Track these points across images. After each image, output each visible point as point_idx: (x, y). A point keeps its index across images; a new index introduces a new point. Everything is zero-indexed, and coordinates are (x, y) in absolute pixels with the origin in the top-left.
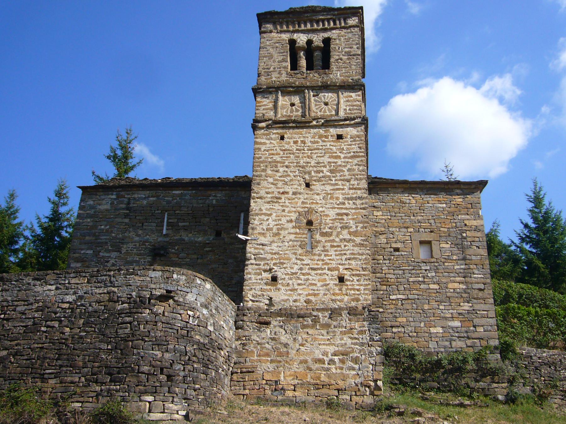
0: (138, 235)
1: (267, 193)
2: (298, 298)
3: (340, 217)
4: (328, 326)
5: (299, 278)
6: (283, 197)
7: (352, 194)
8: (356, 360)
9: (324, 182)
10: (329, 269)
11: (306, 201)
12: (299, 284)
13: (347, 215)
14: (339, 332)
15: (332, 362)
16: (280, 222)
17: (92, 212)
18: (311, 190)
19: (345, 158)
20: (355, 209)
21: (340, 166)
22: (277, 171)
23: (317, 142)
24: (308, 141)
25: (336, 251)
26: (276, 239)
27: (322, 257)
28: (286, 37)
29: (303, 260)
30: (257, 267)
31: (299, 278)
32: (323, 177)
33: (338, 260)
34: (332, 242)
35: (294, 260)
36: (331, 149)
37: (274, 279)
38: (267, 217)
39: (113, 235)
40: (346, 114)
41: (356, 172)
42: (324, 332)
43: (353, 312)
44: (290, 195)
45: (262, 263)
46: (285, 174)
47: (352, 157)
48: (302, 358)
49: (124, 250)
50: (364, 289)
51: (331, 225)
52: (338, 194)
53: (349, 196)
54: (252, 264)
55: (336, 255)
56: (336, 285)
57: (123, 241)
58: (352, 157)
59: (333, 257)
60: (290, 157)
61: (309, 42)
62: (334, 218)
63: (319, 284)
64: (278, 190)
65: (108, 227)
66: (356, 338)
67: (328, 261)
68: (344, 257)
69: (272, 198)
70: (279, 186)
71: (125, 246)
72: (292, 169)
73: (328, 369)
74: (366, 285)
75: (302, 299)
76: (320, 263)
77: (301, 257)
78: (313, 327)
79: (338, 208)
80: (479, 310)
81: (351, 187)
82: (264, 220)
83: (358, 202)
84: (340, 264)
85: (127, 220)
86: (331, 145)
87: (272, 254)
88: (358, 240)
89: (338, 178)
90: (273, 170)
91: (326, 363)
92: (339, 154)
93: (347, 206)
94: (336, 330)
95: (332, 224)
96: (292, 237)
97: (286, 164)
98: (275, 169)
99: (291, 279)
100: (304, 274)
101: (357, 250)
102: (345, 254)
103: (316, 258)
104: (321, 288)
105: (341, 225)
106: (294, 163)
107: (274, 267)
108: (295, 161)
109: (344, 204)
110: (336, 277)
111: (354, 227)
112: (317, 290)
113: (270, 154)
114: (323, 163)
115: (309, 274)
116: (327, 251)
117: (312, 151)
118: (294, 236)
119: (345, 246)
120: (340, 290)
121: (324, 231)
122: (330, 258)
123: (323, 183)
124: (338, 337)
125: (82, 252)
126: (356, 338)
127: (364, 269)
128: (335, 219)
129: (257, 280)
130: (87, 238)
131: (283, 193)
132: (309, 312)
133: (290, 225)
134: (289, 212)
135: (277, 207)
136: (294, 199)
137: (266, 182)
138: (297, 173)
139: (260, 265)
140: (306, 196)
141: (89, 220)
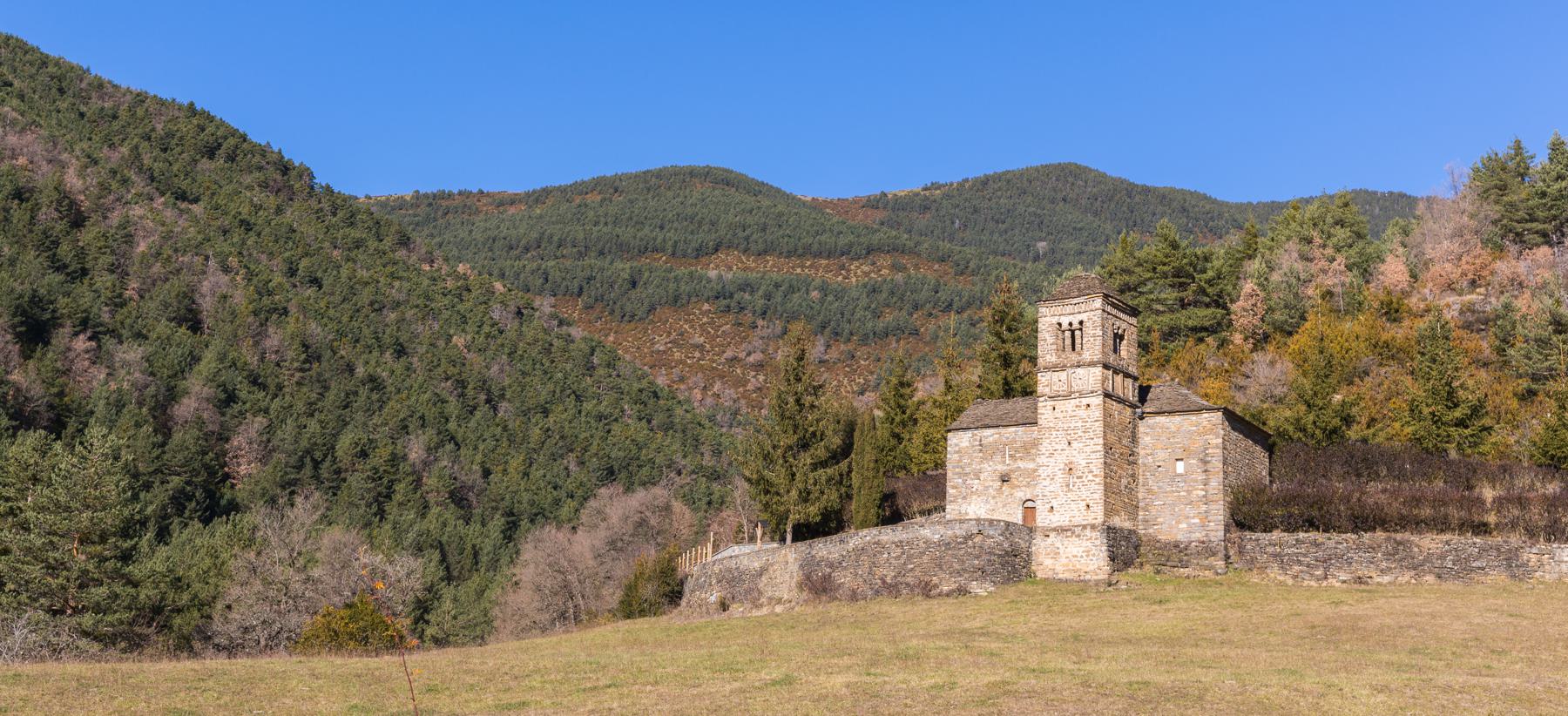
28: (1055, 320)
43: (1093, 527)
52: (1087, 449)
86: (1082, 413)
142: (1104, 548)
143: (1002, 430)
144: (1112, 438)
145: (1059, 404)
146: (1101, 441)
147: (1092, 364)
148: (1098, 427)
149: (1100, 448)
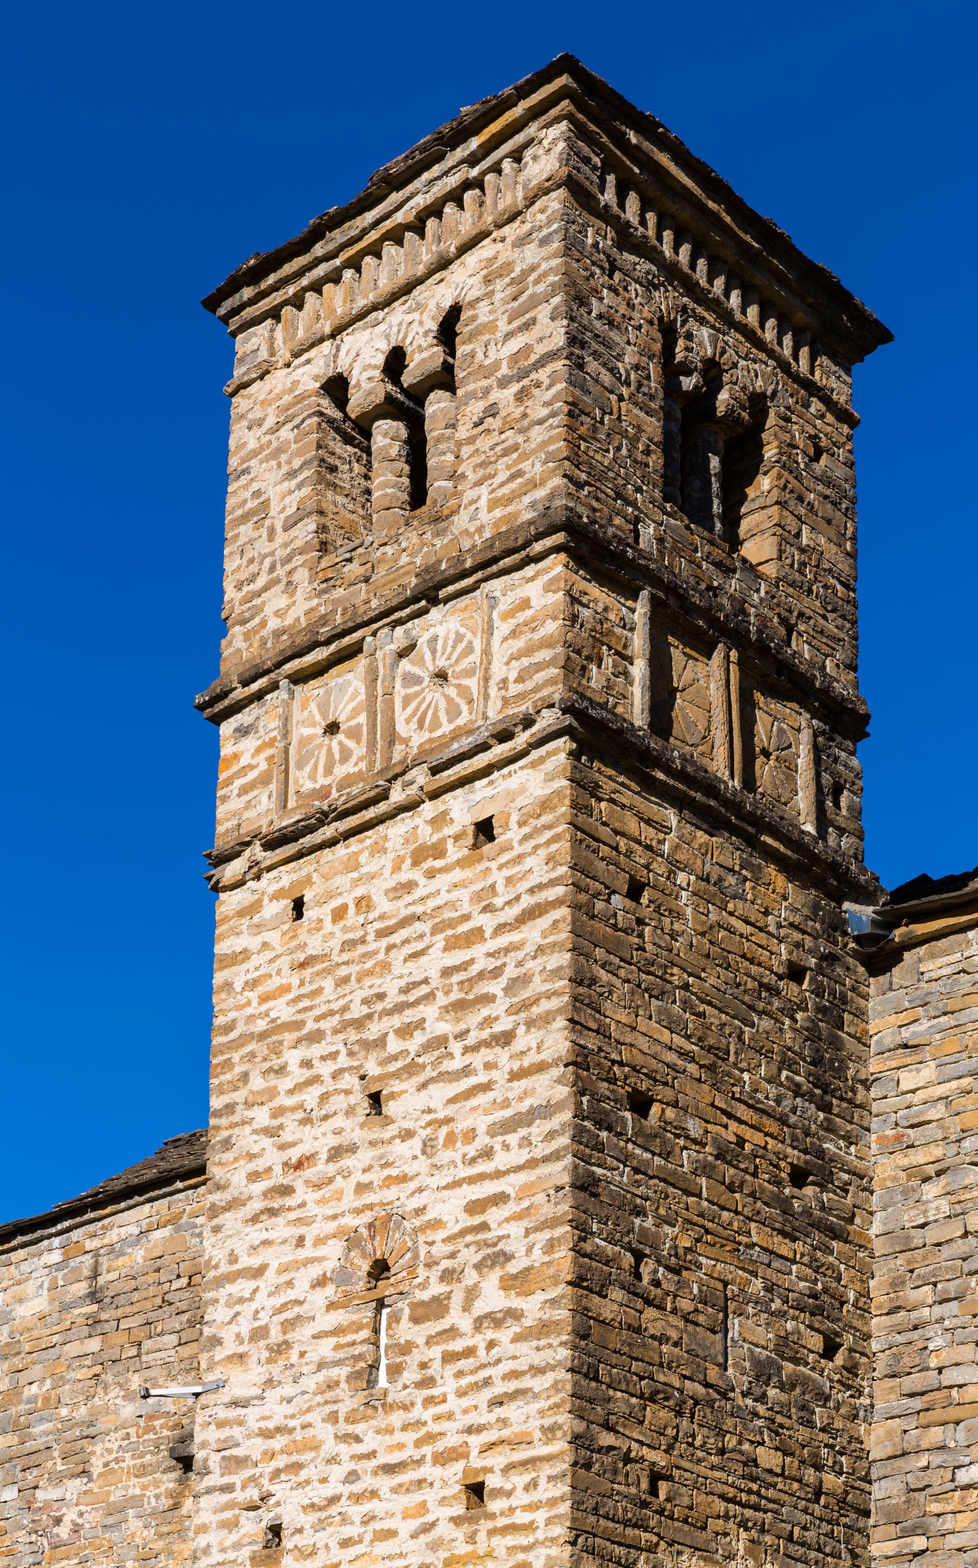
1: (254, 1176)
6: (297, 1180)
7: (521, 1099)
9: (429, 1073)
11: (366, 1178)
12: (346, 1543)
13: (501, 1198)
16: (291, 1295)
18: (389, 1121)
19: (501, 929)
20: (532, 1164)
22: (281, 1071)
24: (377, 890)
25: (460, 1374)
26: (276, 1370)
27: (417, 1412)
28: (309, 375)
29: (358, 1439)
31: (345, 1519)
33: (466, 1412)
34: (446, 1341)
35: (330, 1446)
38: (252, 1284)
40: (506, 702)
41: (538, 986)
44: (321, 1168)
45: (237, 1479)
50: (548, 1522)
51: (445, 1264)
53: (508, 1113)
54: (209, 1491)
55: (461, 1394)
59: (454, 1403)
60: (319, 991)
62: (457, 1229)
63: (406, 1528)
68: (486, 1395)
69: (265, 1194)
70: (287, 1136)
74: (552, 1502)
76: (410, 1437)
79: (471, 1180)
81: (516, 1066)
82: (241, 1301)
83: (539, 1128)
86: (451, 887)
87: (267, 1434)
88: (532, 1306)
89: (471, 1040)
93: (501, 1160)
96: (326, 1348)
97: (310, 1026)
98: (276, 1062)
99: (320, 1526)
100: (357, 1498)
101: (528, 1354)
102: (487, 1382)
103: (397, 1419)
104: (412, 1545)
107: (273, 1489)
109: (487, 1153)
112: (401, 1555)
114: (426, 981)
118: (332, 1341)
119: (491, 1345)
120: (471, 1539)
121: (425, 1296)
127: (550, 1432)
129: (223, 1550)
131: (299, 1166)
134: (320, 1241)
135: (280, 1229)
138: (343, 1061)
144: (648, 1036)
145: (330, 876)
146: (557, 1041)
147: (505, 555)
148: (542, 953)
149: (553, 1087)
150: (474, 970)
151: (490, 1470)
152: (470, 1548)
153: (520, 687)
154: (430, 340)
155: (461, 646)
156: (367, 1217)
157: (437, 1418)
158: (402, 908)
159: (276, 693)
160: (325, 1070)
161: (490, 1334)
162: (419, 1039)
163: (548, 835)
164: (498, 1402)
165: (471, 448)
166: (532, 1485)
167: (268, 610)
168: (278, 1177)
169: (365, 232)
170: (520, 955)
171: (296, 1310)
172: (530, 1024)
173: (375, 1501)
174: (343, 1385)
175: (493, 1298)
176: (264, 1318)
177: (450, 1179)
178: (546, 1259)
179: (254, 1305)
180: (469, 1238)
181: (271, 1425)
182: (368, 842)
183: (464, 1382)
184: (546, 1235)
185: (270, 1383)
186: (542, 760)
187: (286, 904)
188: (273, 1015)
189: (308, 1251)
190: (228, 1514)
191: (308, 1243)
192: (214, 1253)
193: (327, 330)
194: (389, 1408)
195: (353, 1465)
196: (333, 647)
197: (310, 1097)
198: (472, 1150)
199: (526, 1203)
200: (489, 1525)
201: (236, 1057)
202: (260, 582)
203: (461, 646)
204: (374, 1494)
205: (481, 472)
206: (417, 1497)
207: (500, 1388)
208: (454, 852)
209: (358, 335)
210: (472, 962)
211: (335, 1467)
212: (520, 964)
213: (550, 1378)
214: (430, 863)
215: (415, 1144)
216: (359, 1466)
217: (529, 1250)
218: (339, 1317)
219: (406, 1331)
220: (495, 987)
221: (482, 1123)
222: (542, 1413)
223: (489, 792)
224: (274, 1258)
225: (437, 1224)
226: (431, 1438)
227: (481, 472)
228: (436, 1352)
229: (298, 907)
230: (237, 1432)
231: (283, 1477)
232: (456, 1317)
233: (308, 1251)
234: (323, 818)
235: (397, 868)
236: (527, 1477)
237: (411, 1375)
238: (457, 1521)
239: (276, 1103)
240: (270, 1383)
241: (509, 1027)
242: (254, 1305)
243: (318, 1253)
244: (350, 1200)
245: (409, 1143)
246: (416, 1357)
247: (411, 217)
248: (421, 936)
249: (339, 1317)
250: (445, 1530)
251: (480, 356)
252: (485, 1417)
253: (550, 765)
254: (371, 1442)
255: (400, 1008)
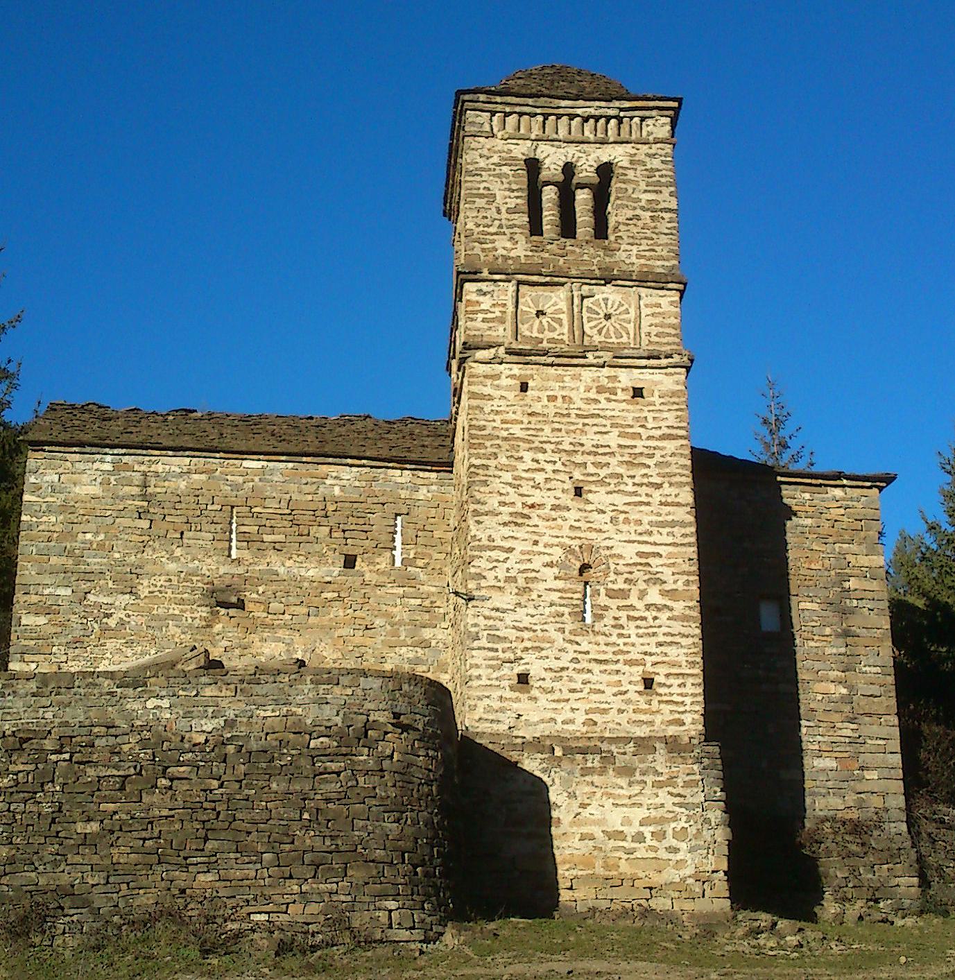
0: (172, 558)
2: (570, 715)
3: (643, 561)
4: (627, 771)
5: (571, 680)
6: (534, 513)
8: (681, 834)
10: (626, 663)
12: (573, 691)
14: (650, 784)
15: (639, 838)
17: (56, 500)
19: (649, 438)
21: (641, 454)
23: (596, 401)
25: (637, 627)
26: (523, 600)
27: (614, 639)
28: (521, 150)
30: (491, 654)
31: (571, 680)
32: (612, 475)
33: (642, 645)
35: (560, 643)
36: (625, 418)
37: (523, 679)
38: (506, 555)
39: (117, 555)
41: (673, 469)
42: (623, 782)
43: (674, 746)
45: (499, 646)
46: (535, 465)
47: (664, 437)
48: (585, 830)
49: (144, 591)
50: (692, 703)
51: (626, 576)
53: (660, 519)
55: (639, 636)
56: (639, 693)
57: (137, 572)
58: (664, 437)
59: (633, 639)
61: (569, 169)
62: (631, 562)
63: (610, 691)
64: (525, 499)
65: (102, 537)
66: (679, 795)
67: (625, 649)
68: (654, 640)
70: (523, 491)
71: (145, 583)
72: (548, 457)
73: (630, 852)
75: (580, 717)
77: (573, 638)
78: (602, 771)
79: (639, 542)
80: (871, 738)
81: (663, 500)
84: (645, 653)
85: (145, 524)
86: (622, 409)
89: (637, 480)
90: (512, 456)
91: (629, 838)
92: (641, 430)
94: (644, 778)
95: (631, 573)
96: (555, 596)
97: (537, 444)
101: (677, 627)
102: (654, 634)
103: (601, 639)
105: (646, 577)
106: (550, 442)
107: (524, 656)
108: (553, 440)
109: (650, 533)
110: (639, 678)
111: (670, 579)
113: (503, 422)
115: (589, 671)
116: (622, 627)
117: (586, 421)
118: (560, 594)
119: (655, 618)
121: (615, 587)
122: (627, 640)
123: (609, 489)
124: (648, 791)
125: (47, 592)
126: (679, 795)
128: (635, 564)
130: (54, 560)
131: (532, 506)
132: (592, 744)
133: (550, 572)
135: (521, 533)
136: (555, 519)
137: (498, 480)
138: (559, 466)
139: (497, 650)
140: (579, 515)
141: (53, 519)
142: (716, 814)
143: (214, 462)
145: (543, 379)
146: (687, 496)
150: (637, 451)
151: (658, 674)
152: (647, 707)
153: (657, 339)
154: (592, 169)
155: (622, 309)
156: (578, 542)
157: (625, 644)
158: (592, 409)
159: (506, 284)
160: (549, 467)
161: (654, 614)
162: (603, 472)
163: (676, 407)
164: (660, 644)
165: (626, 228)
166: (683, 685)
167: (497, 244)
168: (518, 508)
169: (558, 108)
170: (663, 453)
171: (534, 574)
172: (671, 484)
173: (590, 675)
174: (567, 616)
175: (654, 596)
176: (513, 573)
177: (627, 539)
178: (685, 588)
179: (506, 565)
180: (639, 567)
181: (521, 625)
182: (569, 373)
183: (641, 631)
184: (686, 577)
185: (519, 604)
186: (671, 374)
187: (516, 383)
188: (511, 431)
189: (540, 548)
190: (494, 662)
191: (541, 545)
192: (478, 533)
193: (533, 137)
194: (596, 633)
195: (575, 655)
196: (548, 279)
197: (540, 477)
198: (640, 529)
199: (672, 561)
200: (659, 698)
201: (488, 444)
202: (492, 230)
203: (622, 309)
204: (589, 671)
205: (631, 241)
206: (616, 678)
207: (661, 639)
208: (621, 395)
209: (547, 147)
210: (635, 447)
211: (563, 653)
212: (662, 456)
213: (690, 640)
214: (607, 395)
215: (607, 517)
216: (580, 656)
217: (675, 582)
218: (560, 584)
219: (603, 600)
220: (650, 462)
221: (646, 519)
222: (686, 655)
223: (641, 377)
224: (519, 546)
225: (620, 556)
226: (622, 652)
227: (631, 241)
228: (623, 614)
229: (524, 387)
230: (498, 624)
231: (530, 651)
232: (633, 600)
233: (540, 548)
234: (545, 353)
235: (588, 390)
236: (680, 681)
237: (608, 621)
238: (639, 693)
239: (516, 473)
240: (519, 604)
241: (659, 482)
242: (506, 565)
243: (547, 550)
244: (566, 532)
245: (602, 516)
246: (611, 613)
247: (586, 115)
248: (605, 426)
249: (560, 584)
250: (632, 695)
251: (630, 191)
252: (654, 649)
253: (676, 377)
254: (585, 646)
255: (596, 454)
